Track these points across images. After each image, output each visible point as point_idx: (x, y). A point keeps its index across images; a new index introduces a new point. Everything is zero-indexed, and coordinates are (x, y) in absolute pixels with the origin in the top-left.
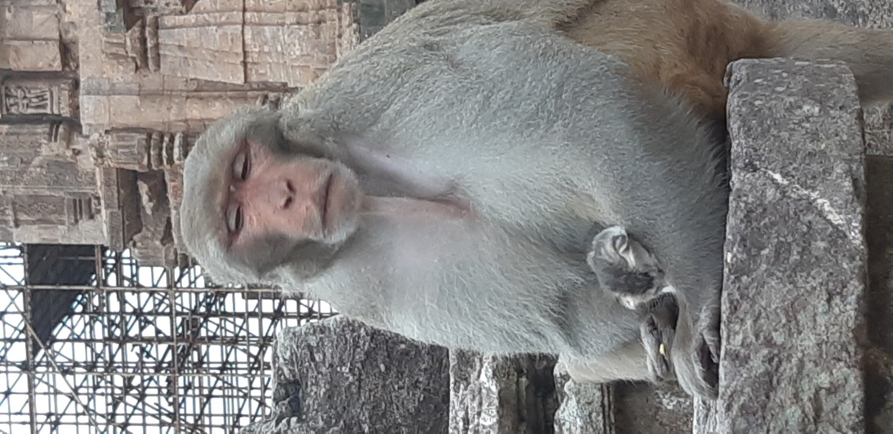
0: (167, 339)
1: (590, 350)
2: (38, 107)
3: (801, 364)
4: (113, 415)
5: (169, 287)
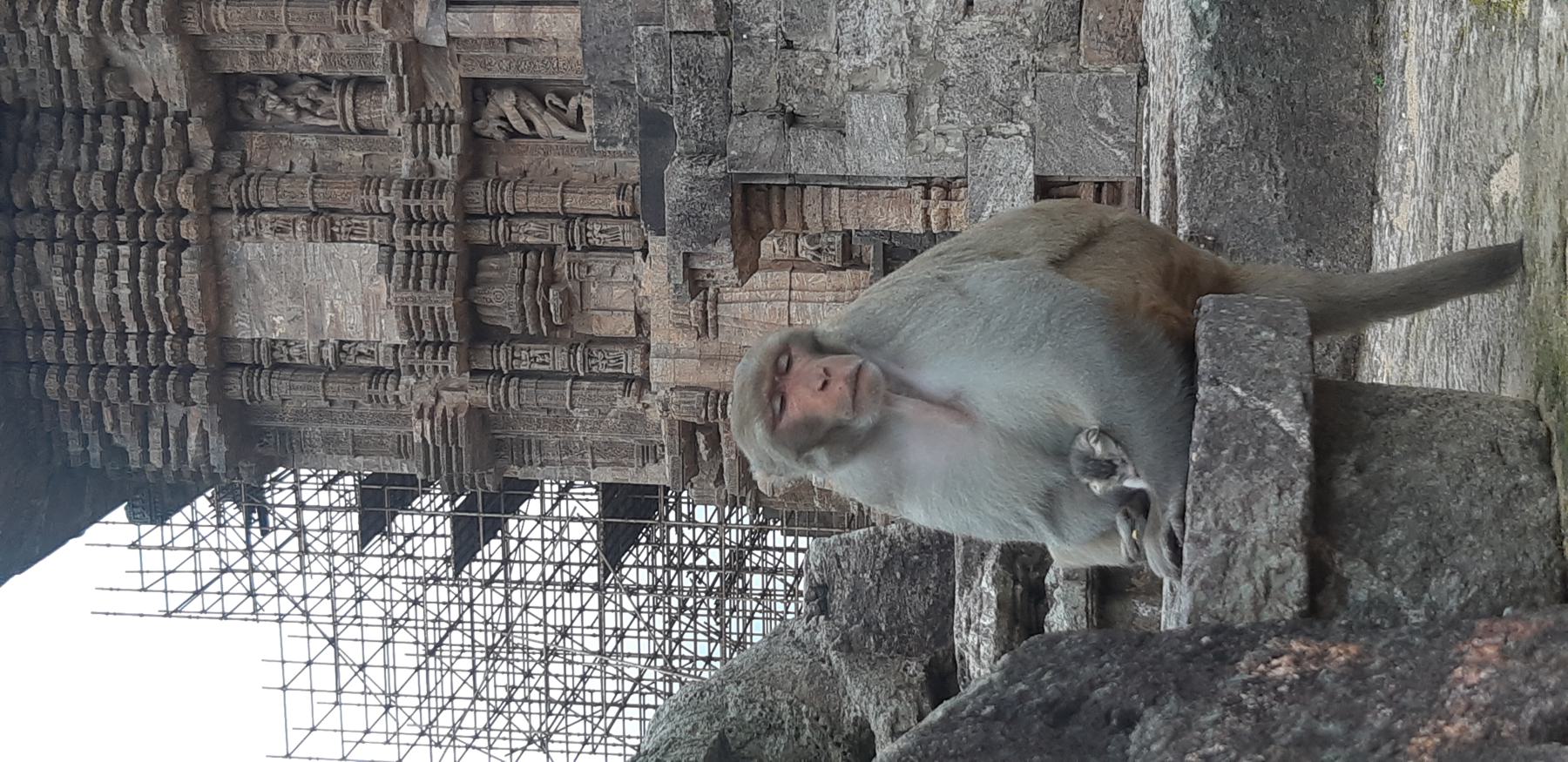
0: (716, 568)
1: (1071, 538)
2: (614, 367)
3: (1254, 548)
4: (670, 631)
5: (720, 523)
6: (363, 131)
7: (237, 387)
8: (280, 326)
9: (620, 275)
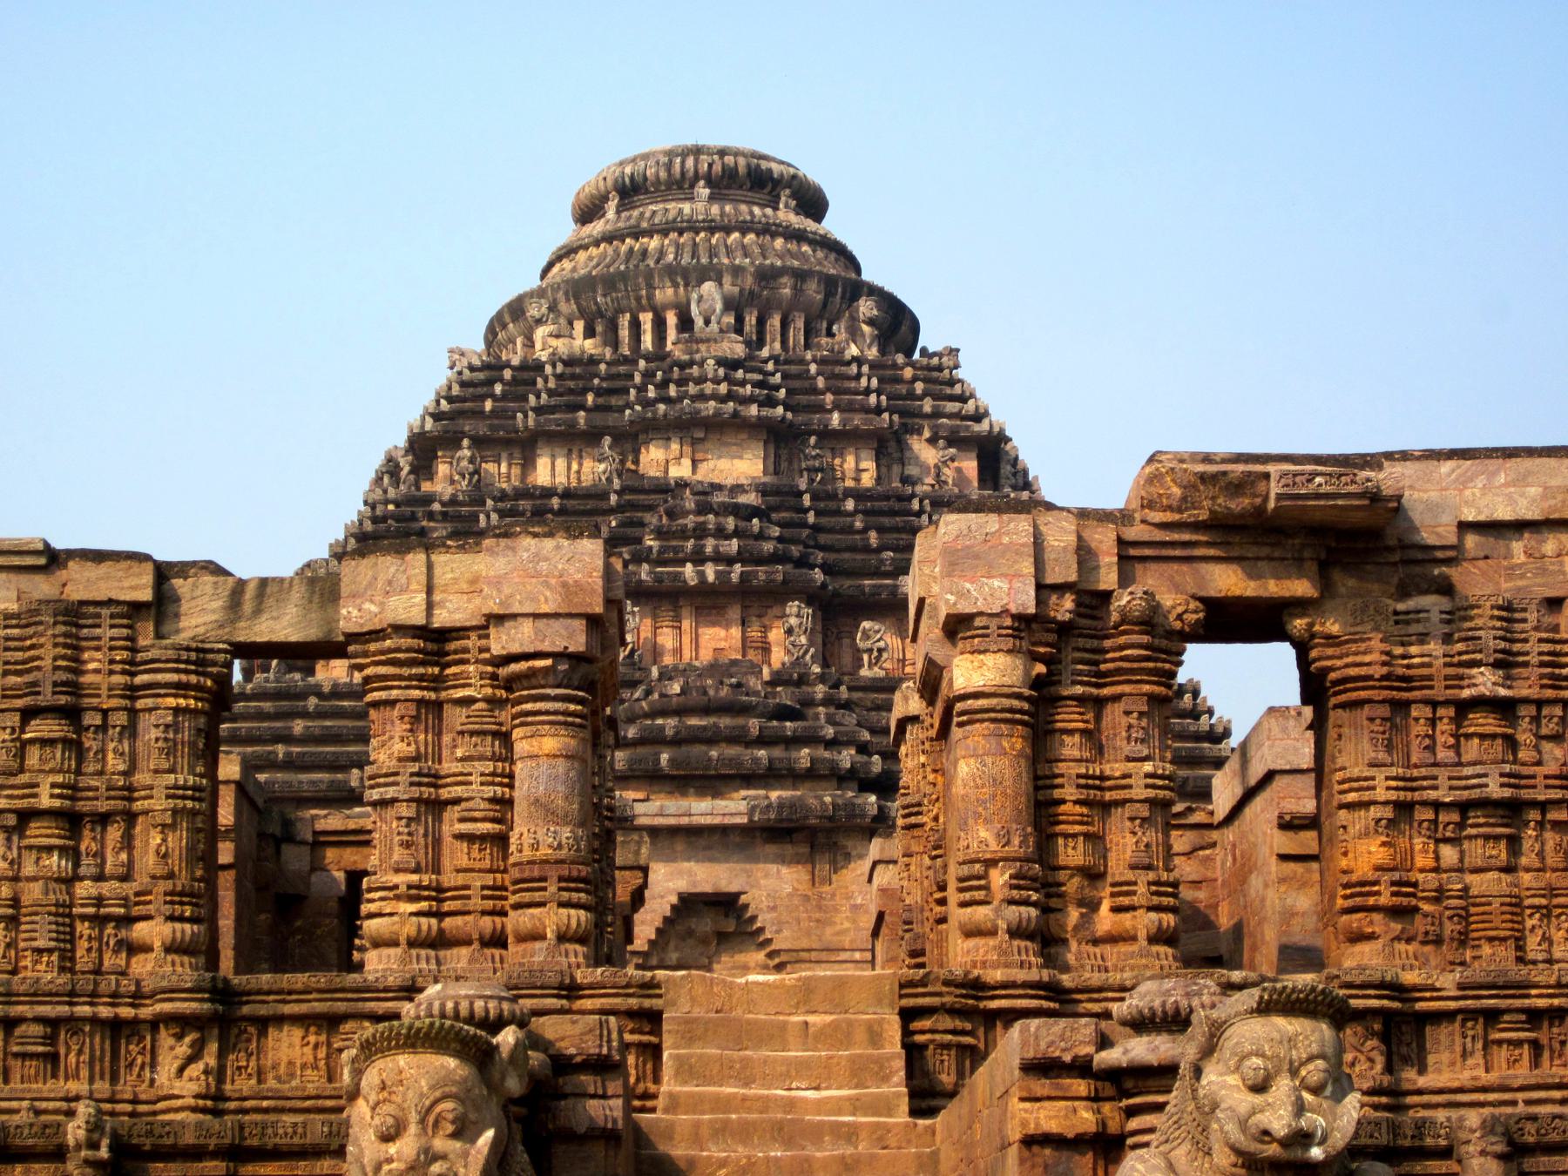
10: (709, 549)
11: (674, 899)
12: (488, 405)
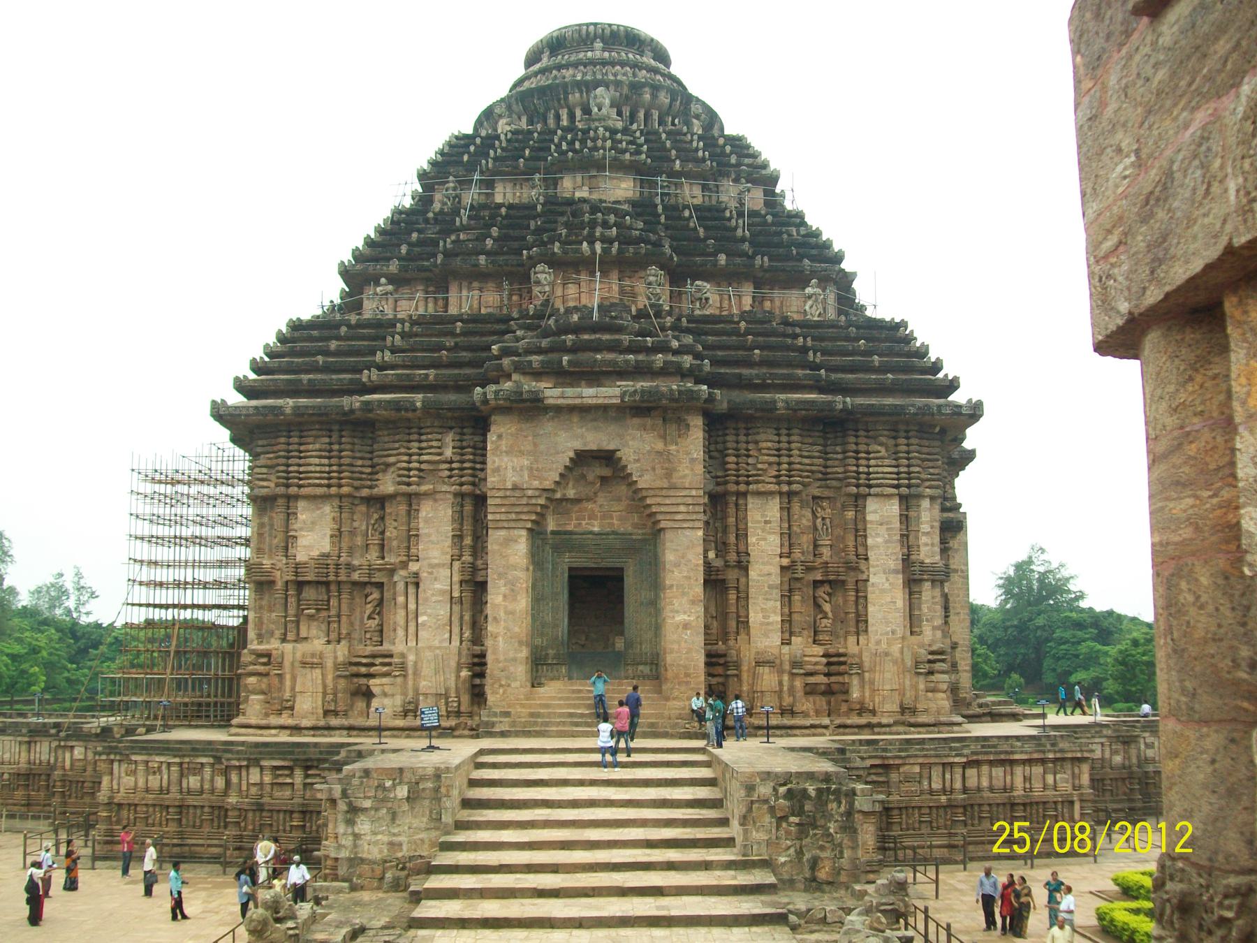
6: (367, 545)
7: (281, 501)
8: (302, 517)
9: (320, 633)
10: (598, 234)
11: (572, 454)
12: (466, 158)
